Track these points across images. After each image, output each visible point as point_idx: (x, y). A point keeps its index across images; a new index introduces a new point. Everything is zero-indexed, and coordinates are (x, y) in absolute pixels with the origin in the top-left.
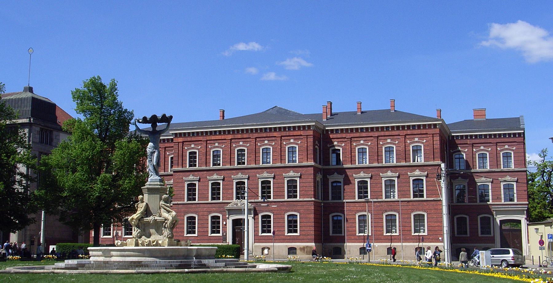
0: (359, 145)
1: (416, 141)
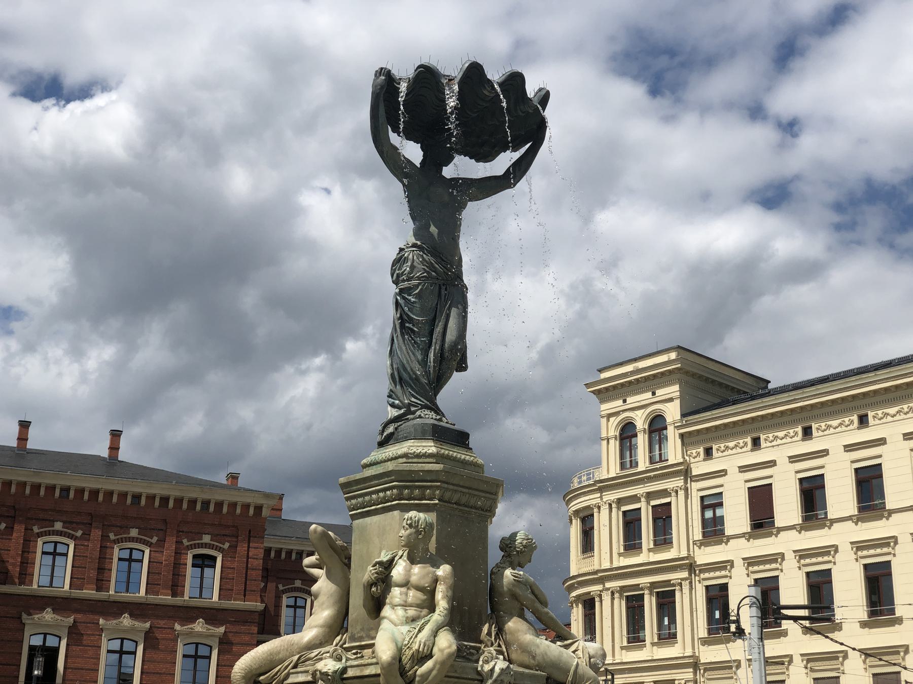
0: (49, 533)
1: (206, 544)
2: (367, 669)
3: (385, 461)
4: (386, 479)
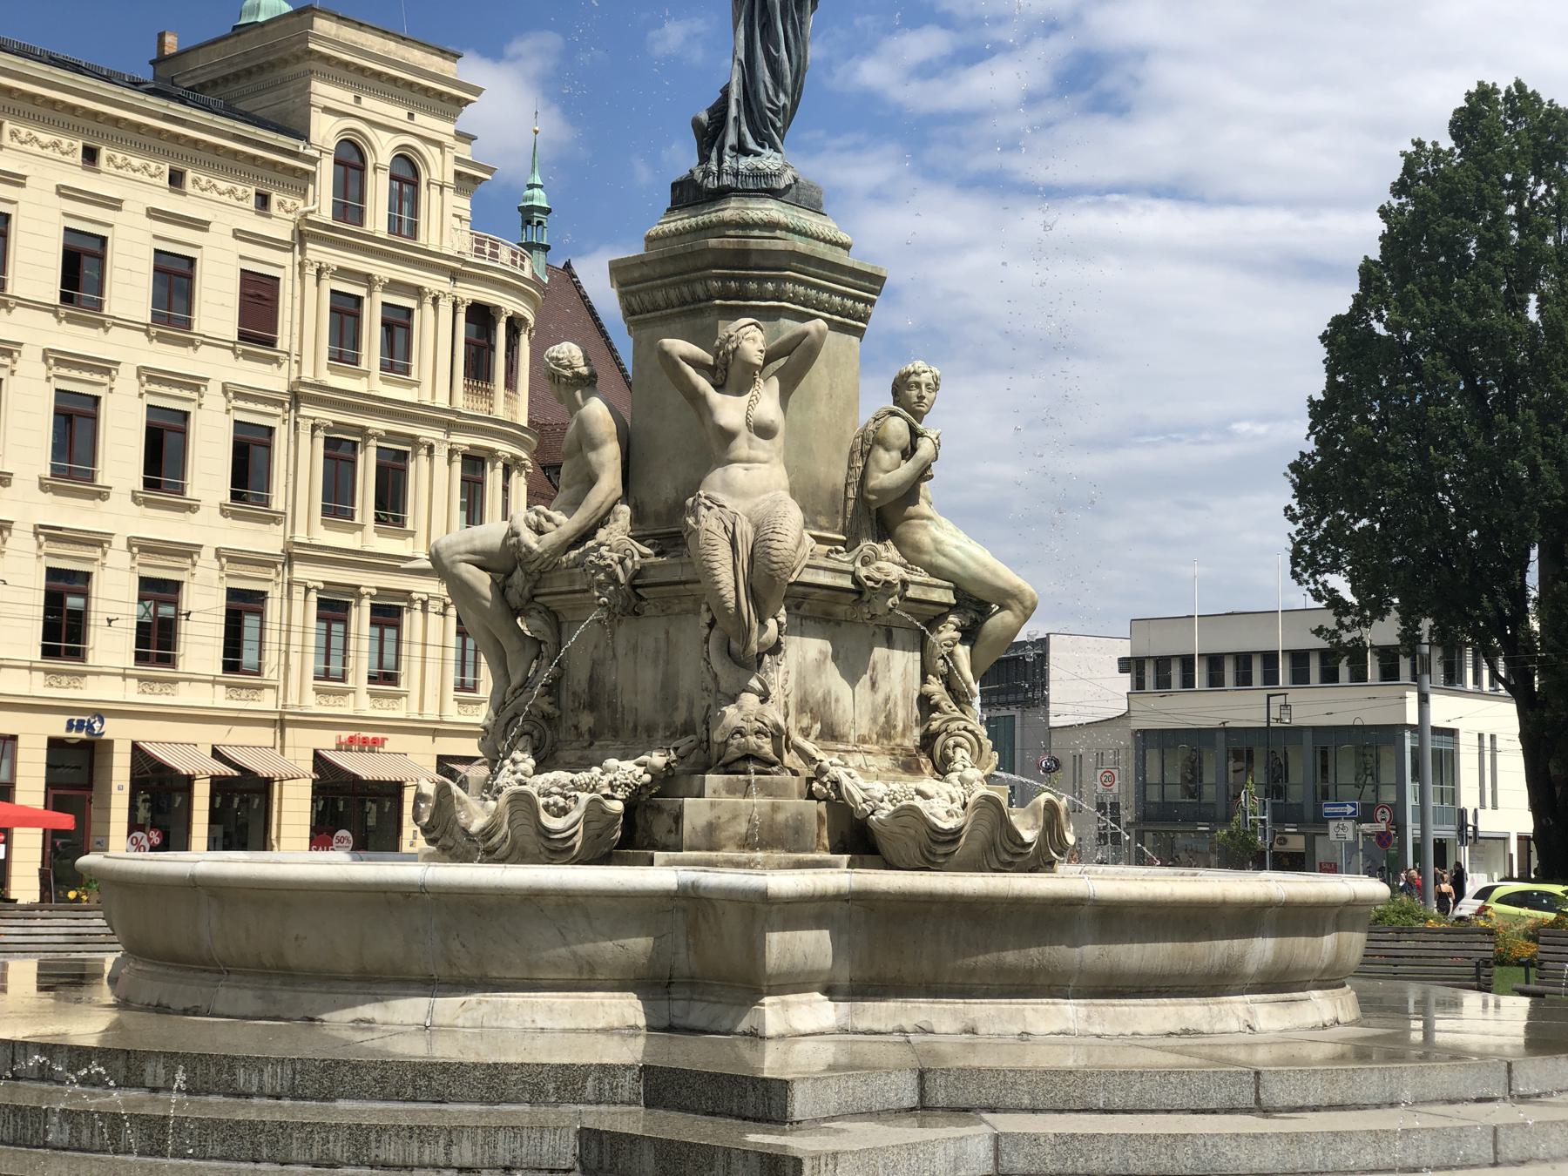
2: (932, 592)
3: (818, 239)
4: (867, 284)
